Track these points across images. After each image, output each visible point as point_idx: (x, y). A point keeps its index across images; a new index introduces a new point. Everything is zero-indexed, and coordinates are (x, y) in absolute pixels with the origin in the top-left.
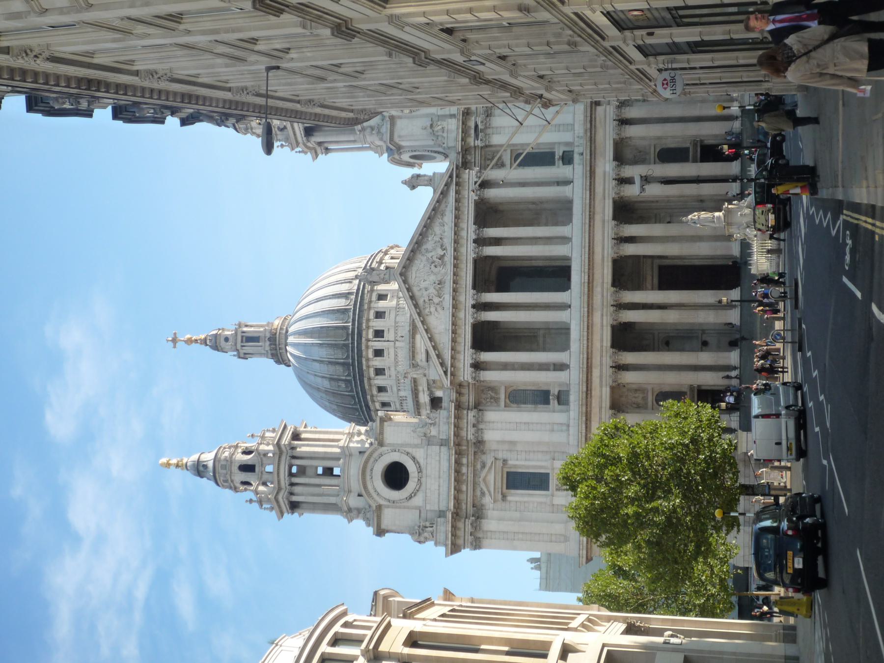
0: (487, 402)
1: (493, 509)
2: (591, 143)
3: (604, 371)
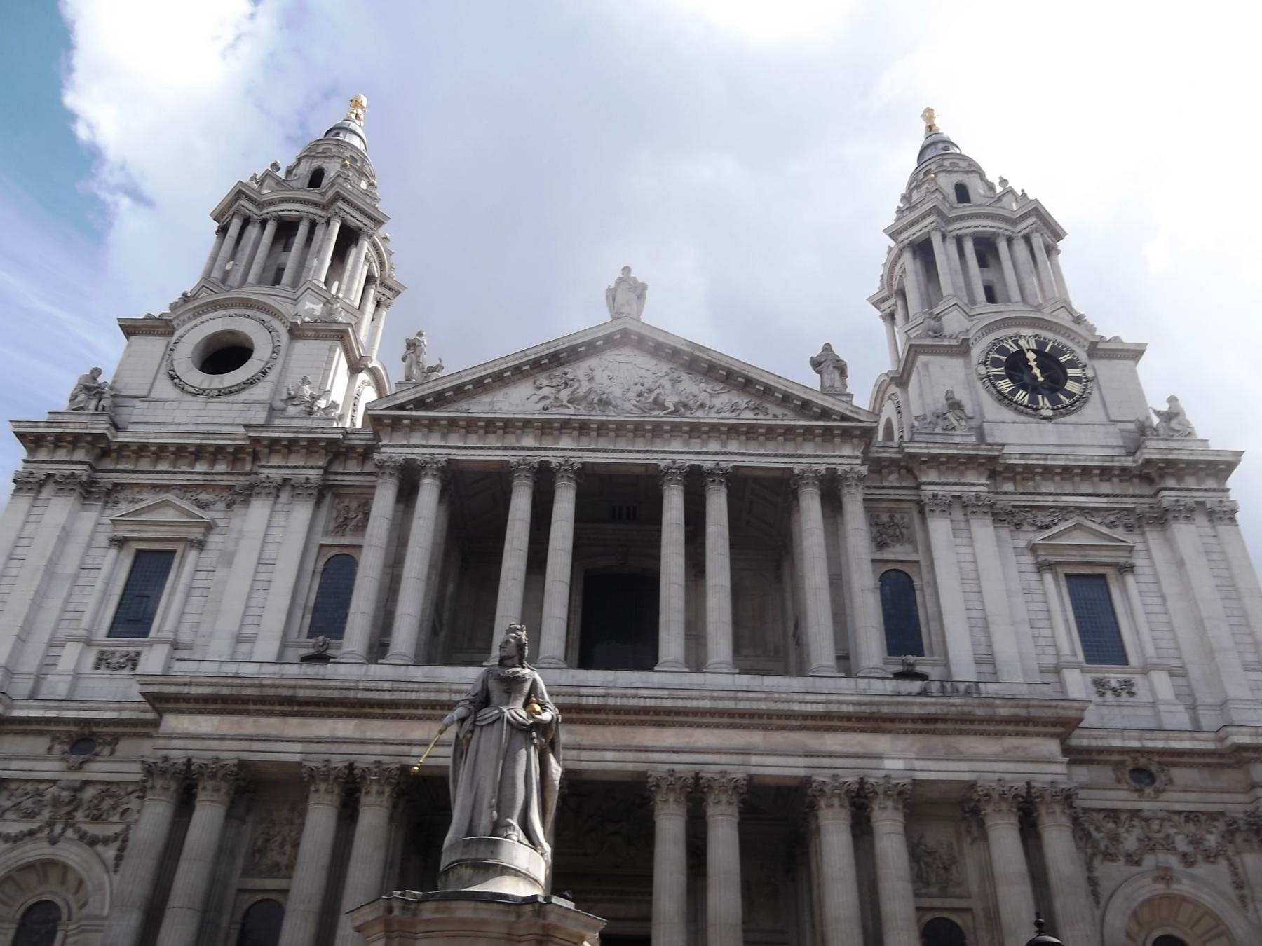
0: (339, 511)
1: (98, 524)
2: (955, 721)
3: (345, 748)
